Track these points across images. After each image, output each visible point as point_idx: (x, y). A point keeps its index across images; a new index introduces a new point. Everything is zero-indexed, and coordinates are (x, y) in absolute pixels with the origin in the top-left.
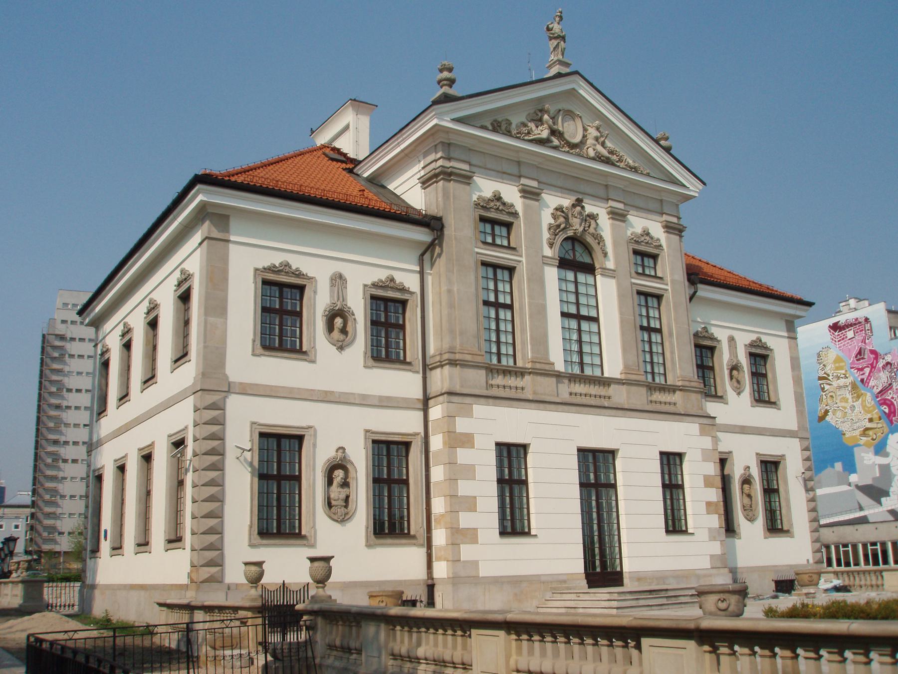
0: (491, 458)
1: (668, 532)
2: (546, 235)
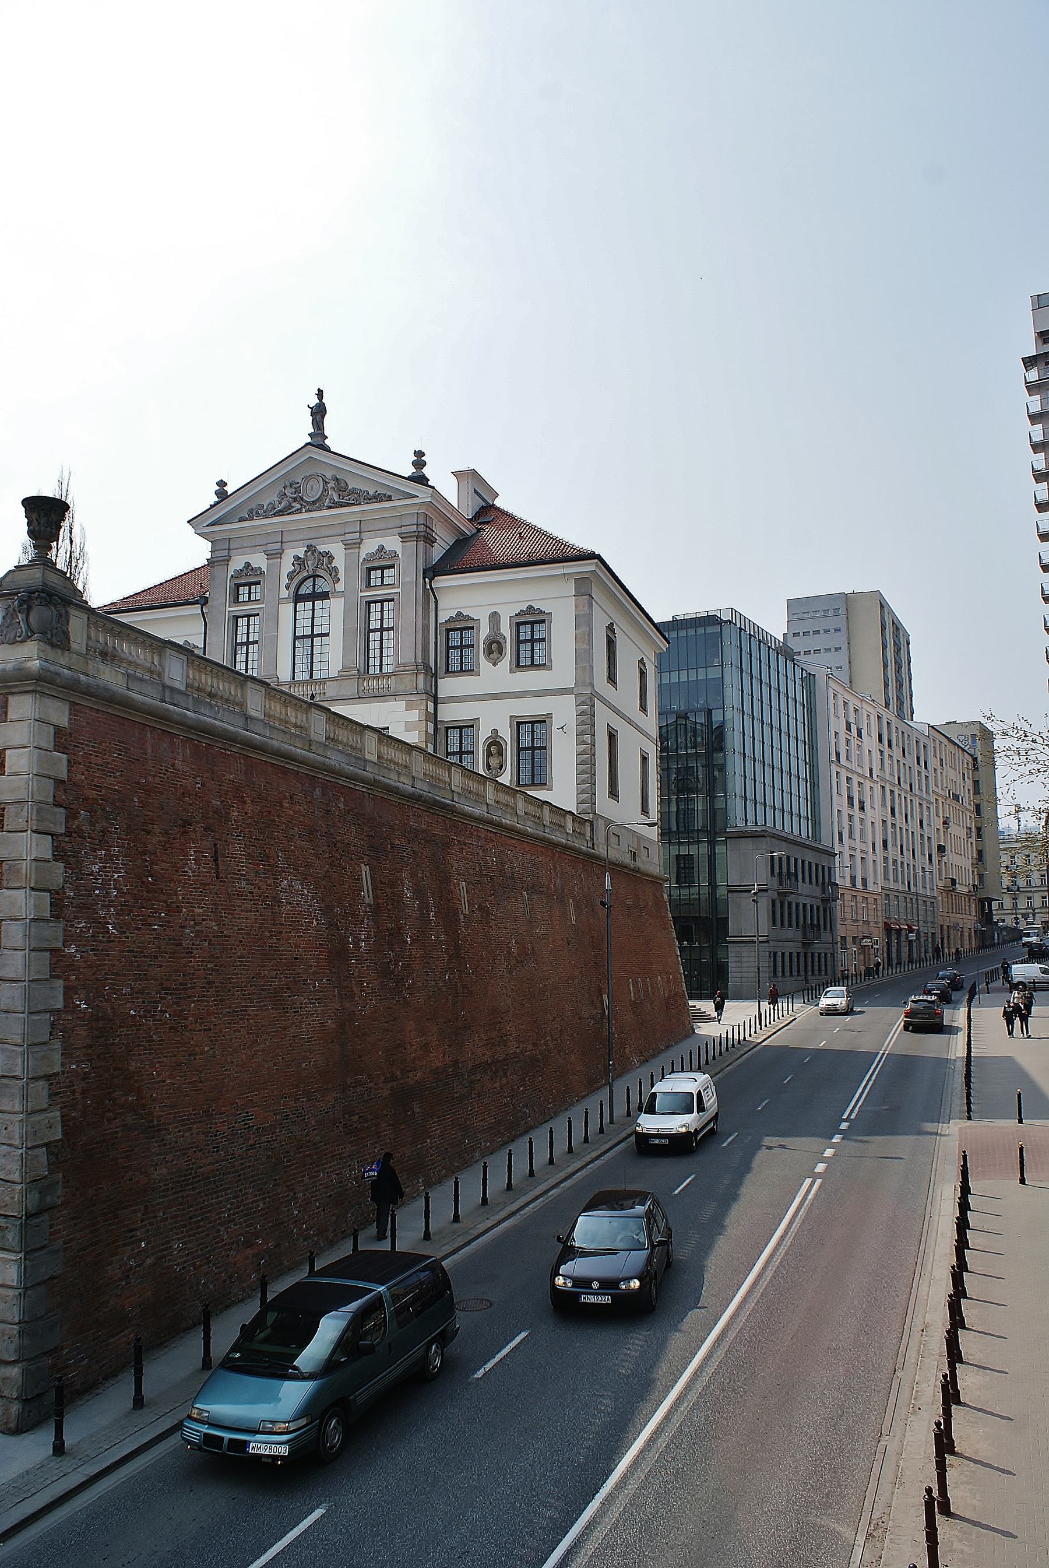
2: (285, 581)
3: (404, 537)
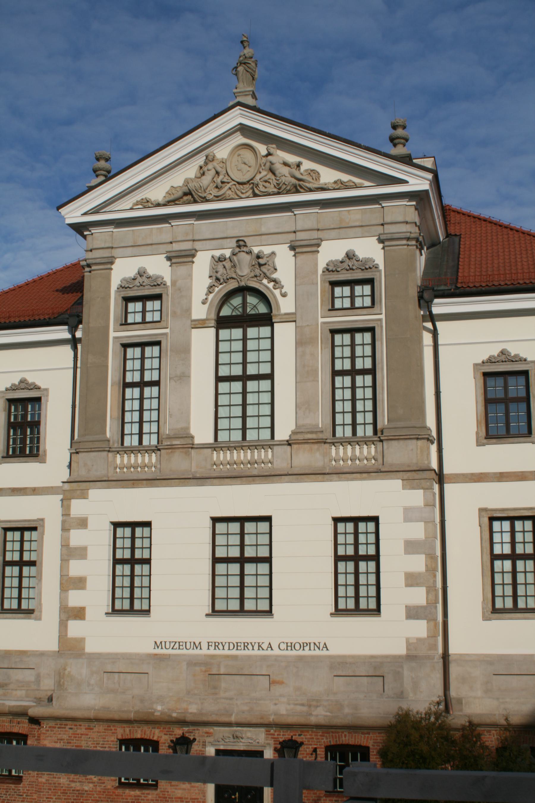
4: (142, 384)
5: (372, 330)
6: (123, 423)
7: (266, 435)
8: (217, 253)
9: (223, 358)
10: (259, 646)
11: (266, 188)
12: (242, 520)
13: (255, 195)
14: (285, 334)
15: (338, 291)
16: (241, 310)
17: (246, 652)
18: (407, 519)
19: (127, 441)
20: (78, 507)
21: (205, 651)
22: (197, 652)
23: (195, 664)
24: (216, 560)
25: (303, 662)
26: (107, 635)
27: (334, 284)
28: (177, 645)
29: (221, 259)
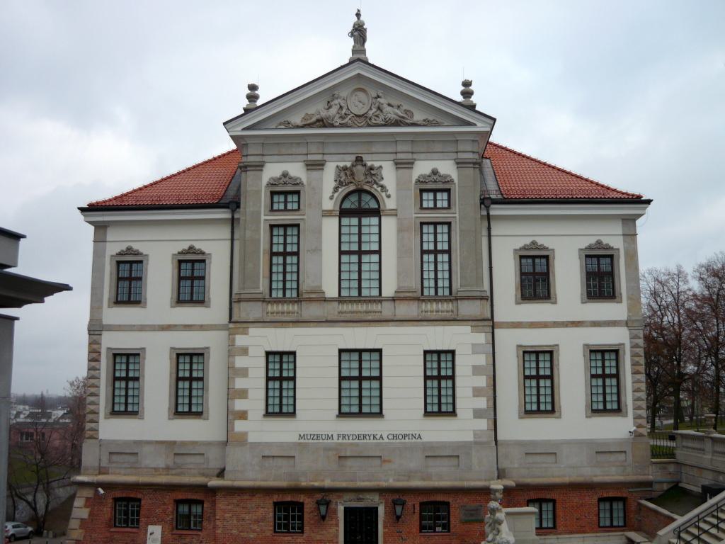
0: (263, 361)
1: (427, 414)
3: (460, 164)
4: (285, 254)
5: (449, 224)
6: (271, 281)
7: (375, 293)
8: (342, 164)
9: (344, 238)
10: (374, 437)
11: (375, 120)
12: (360, 351)
13: (369, 126)
14: (389, 224)
15: (425, 196)
16: (357, 204)
17: (365, 441)
18: (474, 352)
19: (274, 295)
20: (240, 340)
21: (335, 440)
22: (330, 441)
23: (330, 449)
24: (341, 379)
25: (406, 444)
26: (263, 431)
27: (422, 191)
28: (316, 437)
29: (345, 169)
